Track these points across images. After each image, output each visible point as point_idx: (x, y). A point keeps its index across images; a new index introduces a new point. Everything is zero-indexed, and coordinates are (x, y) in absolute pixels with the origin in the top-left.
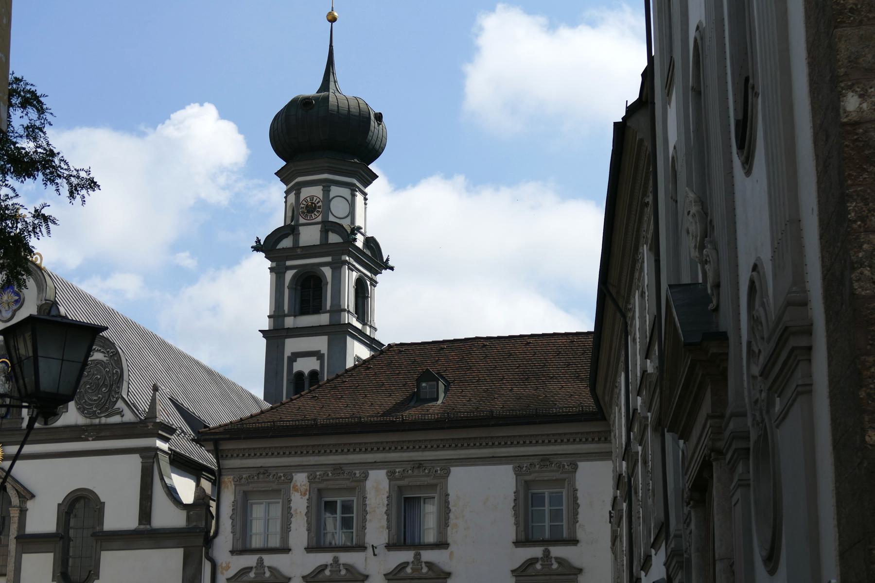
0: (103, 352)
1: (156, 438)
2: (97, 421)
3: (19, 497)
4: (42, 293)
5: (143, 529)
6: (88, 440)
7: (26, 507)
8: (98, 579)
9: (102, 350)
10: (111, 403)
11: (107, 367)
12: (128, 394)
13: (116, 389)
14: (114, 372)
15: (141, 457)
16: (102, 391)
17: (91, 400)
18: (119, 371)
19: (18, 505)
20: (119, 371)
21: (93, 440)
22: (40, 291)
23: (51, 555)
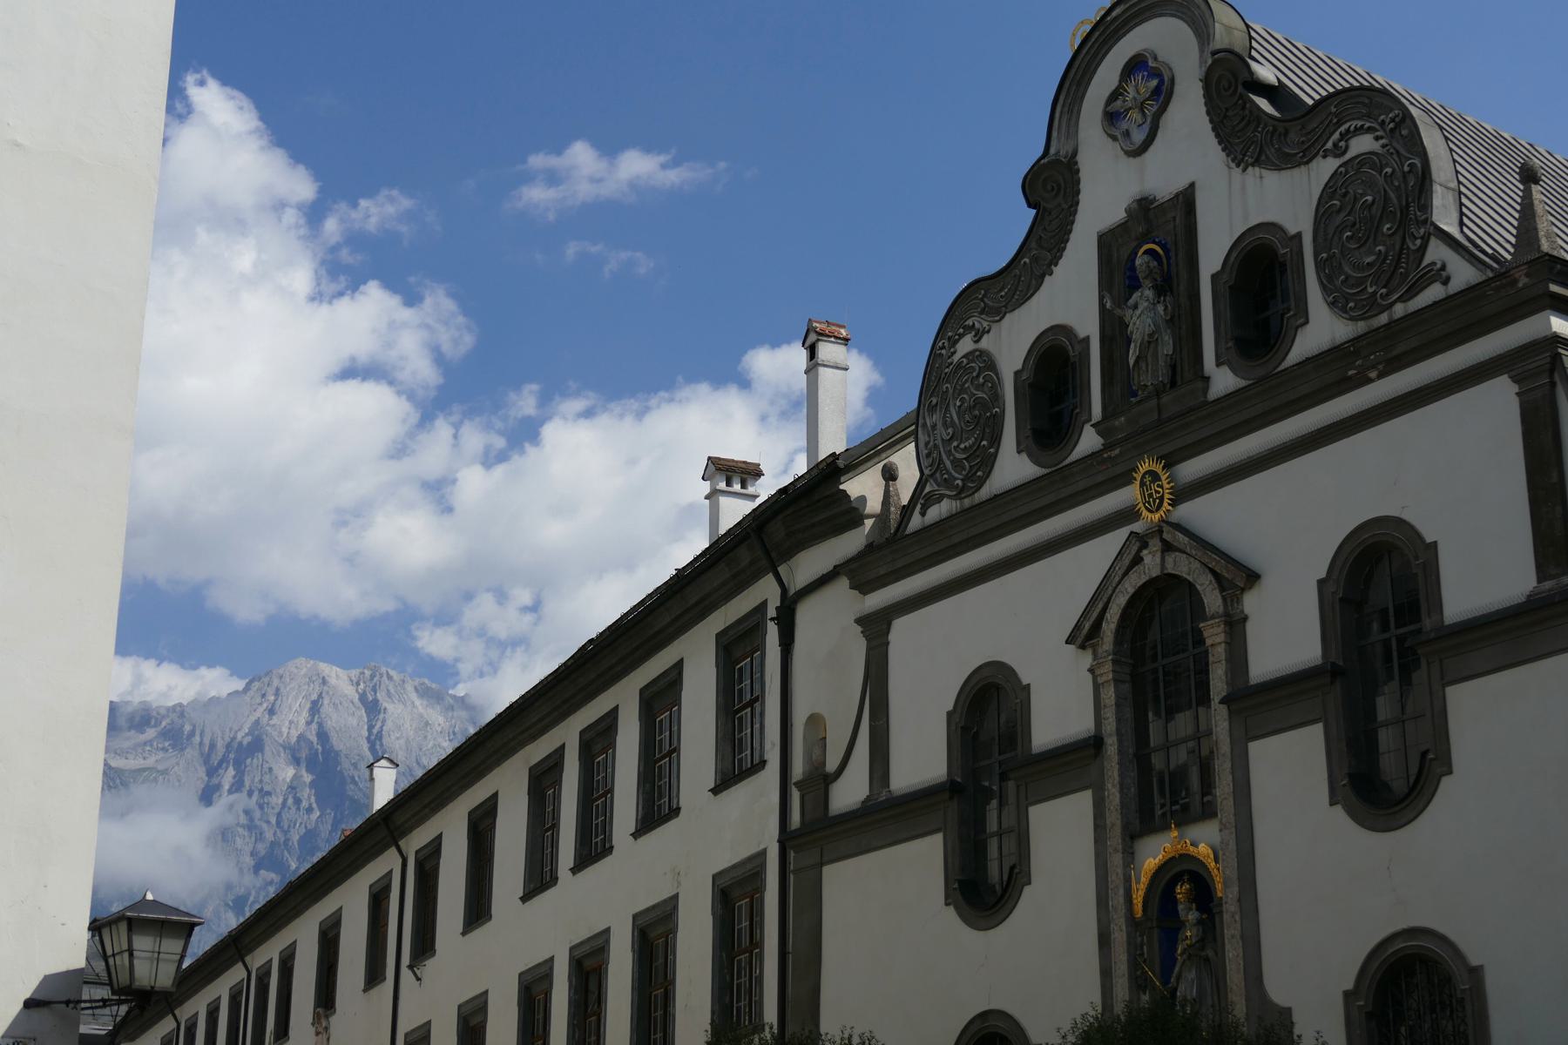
0: (1370, 130)
1: (1548, 311)
2: (1383, 319)
3: (1222, 589)
4: (1209, 44)
5: (1549, 590)
6: (1370, 381)
7: (1242, 611)
8: (1450, 772)
9: (1368, 125)
10: (1411, 258)
11: (1387, 165)
12: (1462, 224)
13: (1419, 213)
14: (1406, 169)
15: (1515, 380)
16: (1383, 234)
17: (1358, 267)
18: (1417, 161)
19: (1221, 610)
20: (1417, 161)
21: (1381, 376)
22: (1203, 44)
23: (1317, 731)
